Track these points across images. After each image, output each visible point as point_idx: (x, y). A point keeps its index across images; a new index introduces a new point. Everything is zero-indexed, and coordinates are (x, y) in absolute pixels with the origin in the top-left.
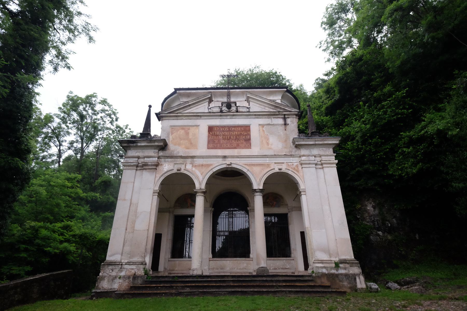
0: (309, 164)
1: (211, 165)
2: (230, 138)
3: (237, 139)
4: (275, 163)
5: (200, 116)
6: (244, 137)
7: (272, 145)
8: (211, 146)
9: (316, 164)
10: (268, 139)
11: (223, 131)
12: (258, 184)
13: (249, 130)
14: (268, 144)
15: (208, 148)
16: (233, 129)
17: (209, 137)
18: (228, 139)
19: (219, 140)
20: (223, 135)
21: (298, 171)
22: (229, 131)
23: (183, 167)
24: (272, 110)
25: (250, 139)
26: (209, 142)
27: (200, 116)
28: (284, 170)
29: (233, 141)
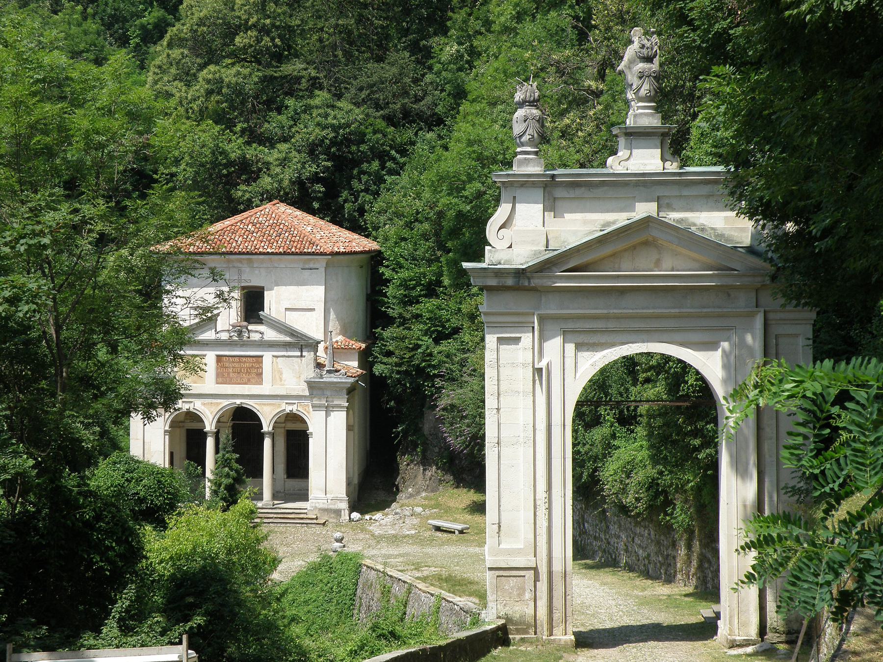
0: (319, 407)
1: (220, 403)
2: (241, 371)
3: (248, 373)
4: (286, 403)
5: (207, 344)
6: (256, 370)
7: (285, 381)
8: (220, 380)
9: (326, 407)
10: (281, 374)
11: (233, 362)
12: (266, 427)
13: (262, 362)
14: (281, 380)
15: (217, 383)
16: (244, 359)
17: (217, 368)
18: (238, 373)
19: (229, 373)
20: (233, 367)
21: (308, 412)
22: (240, 362)
23: (191, 406)
24: (288, 339)
25: (262, 373)
26: (218, 375)
27: (207, 344)
28: (295, 411)
29: (244, 375)
